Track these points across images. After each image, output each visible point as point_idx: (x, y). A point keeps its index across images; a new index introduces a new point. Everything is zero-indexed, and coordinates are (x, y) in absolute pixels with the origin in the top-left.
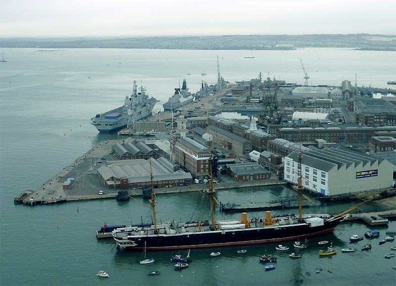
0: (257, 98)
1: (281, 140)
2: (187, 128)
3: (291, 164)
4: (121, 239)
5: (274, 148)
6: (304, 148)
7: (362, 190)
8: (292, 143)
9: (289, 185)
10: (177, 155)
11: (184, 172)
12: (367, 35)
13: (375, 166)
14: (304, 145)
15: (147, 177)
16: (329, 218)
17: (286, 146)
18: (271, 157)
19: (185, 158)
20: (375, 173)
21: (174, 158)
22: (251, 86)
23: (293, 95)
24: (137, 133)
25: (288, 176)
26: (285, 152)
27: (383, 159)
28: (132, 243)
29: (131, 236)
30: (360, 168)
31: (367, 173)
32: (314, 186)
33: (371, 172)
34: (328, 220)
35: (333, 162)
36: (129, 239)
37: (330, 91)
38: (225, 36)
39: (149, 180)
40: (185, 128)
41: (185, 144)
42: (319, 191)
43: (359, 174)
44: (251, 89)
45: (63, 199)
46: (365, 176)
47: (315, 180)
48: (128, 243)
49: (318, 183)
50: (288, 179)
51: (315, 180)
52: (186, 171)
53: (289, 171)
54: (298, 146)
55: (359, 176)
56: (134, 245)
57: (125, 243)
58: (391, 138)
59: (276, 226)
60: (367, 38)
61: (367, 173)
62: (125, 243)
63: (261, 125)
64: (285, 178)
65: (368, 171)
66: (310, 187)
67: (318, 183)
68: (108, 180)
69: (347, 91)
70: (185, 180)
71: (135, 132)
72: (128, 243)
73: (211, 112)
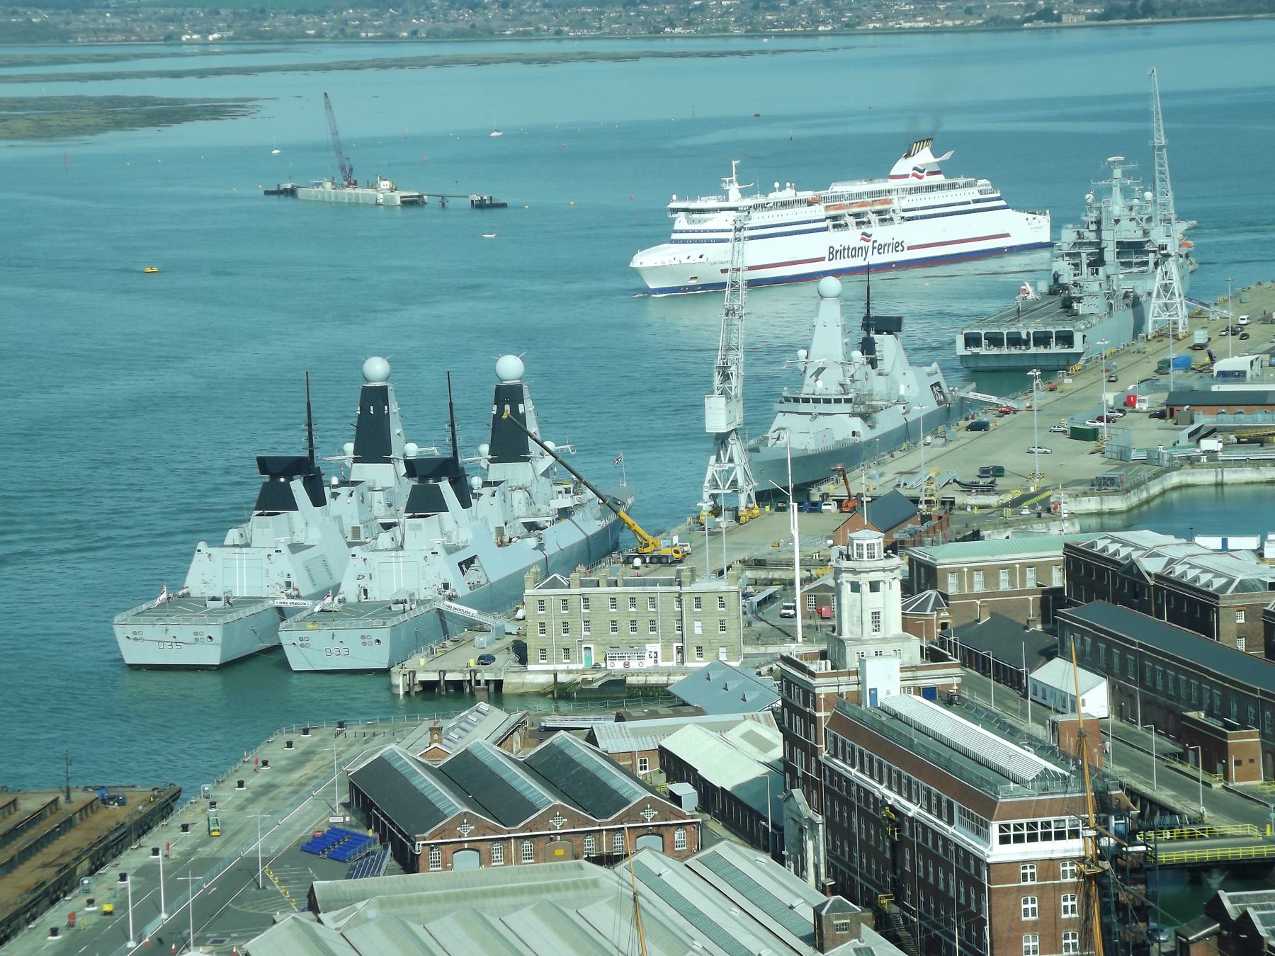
2: (907, 625)
24: (538, 675)
73: (1091, 504)
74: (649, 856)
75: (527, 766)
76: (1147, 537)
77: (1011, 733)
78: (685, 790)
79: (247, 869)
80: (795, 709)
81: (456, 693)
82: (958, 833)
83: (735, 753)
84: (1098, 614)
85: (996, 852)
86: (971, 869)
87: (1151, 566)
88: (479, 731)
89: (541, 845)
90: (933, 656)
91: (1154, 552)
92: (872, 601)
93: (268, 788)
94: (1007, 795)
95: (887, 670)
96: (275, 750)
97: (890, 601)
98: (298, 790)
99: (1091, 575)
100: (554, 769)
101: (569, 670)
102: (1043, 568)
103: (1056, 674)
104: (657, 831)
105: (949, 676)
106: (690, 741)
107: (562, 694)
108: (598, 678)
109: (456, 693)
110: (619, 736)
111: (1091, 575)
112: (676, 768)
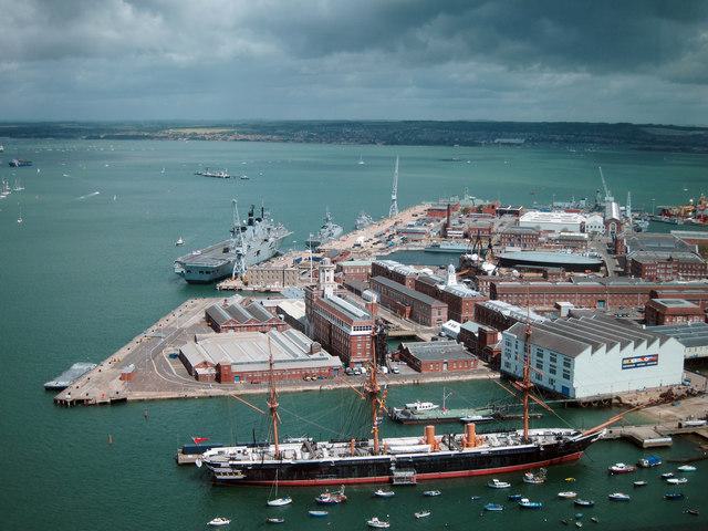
0: (459, 229)
1: (497, 302)
2: (335, 279)
3: (514, 344)
4: (218, 466)
5: (483, 315)
6: (537, 318)
7: (631, 389)
8: (515, 309)
9: (508, 378)
10: (317, 327)
11: (327, 355)
12: (651, 126)
13: (655, 348)
14: (537, 312)
15: (265, 362)
16: (574, 435)
17: (506, 313)
18: (480, 331)
19: (330, 330)
20: (654, 360)
21: (312, 329)
22: (448, 210)
23: (521, 225)
25: (508, 365)
26: (502, 323)
27: (669, 337)
28: (236, 474)
29: (235, 463)
30: (630, 351)
31: (640, 360)
32: (552, 381)
33: (647, 359)
34: (571, 439)
35: (585, 341)
36: (233, 466)
37: (584, 220)
38: (406, 122)
39: (267, 367)
40: (332, 280)
41: (331, 309)
42: (559, 390)
43: (627, 362)
44: (449, 215)
45: (121, 397)
46: (636, 365)
47: (553, 371)
48: (231, 474)
49: (545, 373)
50: (507, 370)
51: (553, 371)
52: (333, 353)
53: (509, 356)
54: (525, 313)
55: (627, 365)
56: (240, 476)
57: (225, 474)
58: (682, 300)
59: (483, 449)
60: (649, 130)
61: (640, 360)
62: (225, 474)
63: (463, 276)
64: (503, 367)
65: (643, 357)
66: (545, 383)
67: (545, 373)
68: (197, 366)
69: (613, 219)
70: (331, 368)
71: (246, 284)
72: (231, 474)
73: (379, 254)
74: (274, 331)
75: (247, 310)
76: (390, 262)
77: (358, 306)
78: (282, 316)
79: (181, 331)
80: (309, 298)
81: (233, 291)
82: (345, 328)
83: (297, 309)
84: (379, 279)
85: (353, 333)
86: (348, 338)
87: (391, 268)
88: (236, 300)
89: (249, 328)
90: (340, 287)
91: (392, 265)
92: (327, 274)
93: (186, 312)
94: (356, 320)
95: (330, 290)
96: (189, 303)
97: (331, 275)
98: (194, 314)
99: (377, 270)
100: (252, 310)
101: (256, 287)
102: (365, 267)
103: (367, 293)
104: (276, 326)
105: (345, 291)
106: (285, 305)
107: (256, 293)
108: (264, 289)
109: (233, 291)
110: (270, 303)
111: (377, 270)
112: (279, 310)
